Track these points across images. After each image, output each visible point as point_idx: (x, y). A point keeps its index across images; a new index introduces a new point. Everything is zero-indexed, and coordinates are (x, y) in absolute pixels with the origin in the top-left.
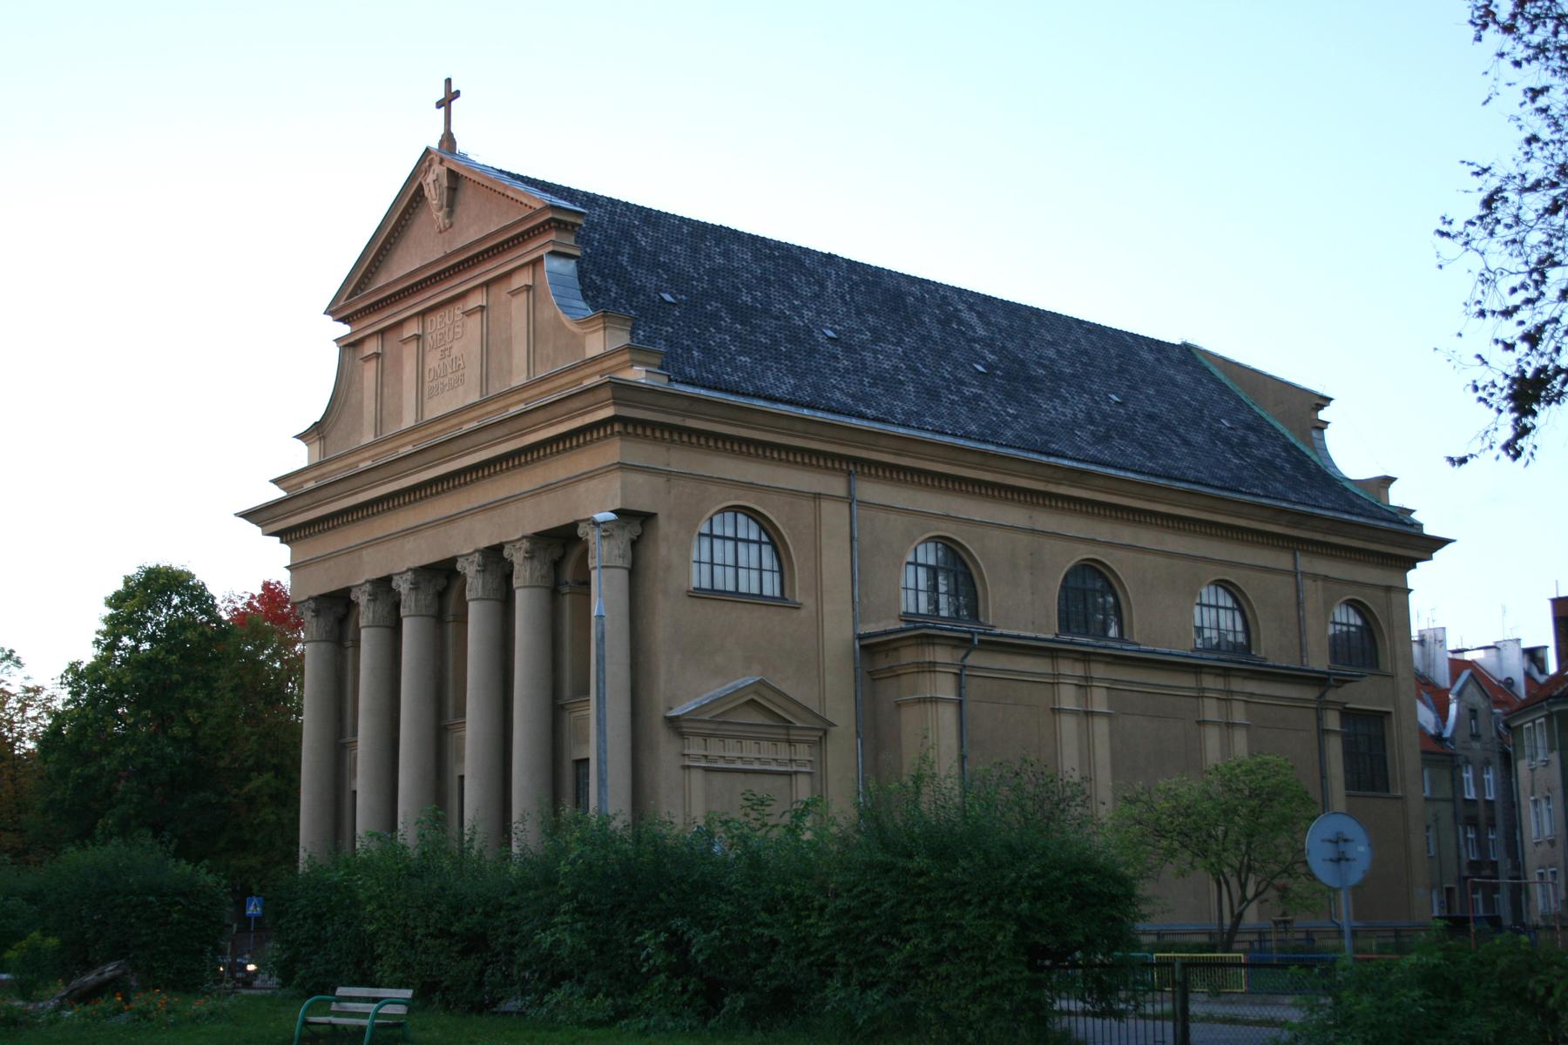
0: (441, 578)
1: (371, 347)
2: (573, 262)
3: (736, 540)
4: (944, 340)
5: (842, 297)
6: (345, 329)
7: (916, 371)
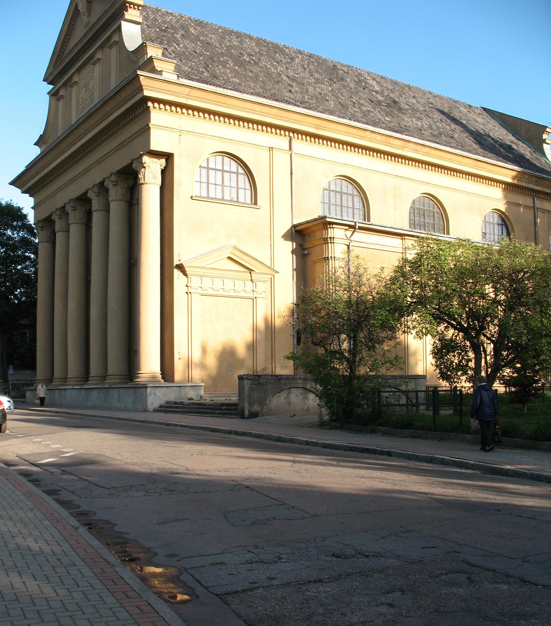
0: (83, 200)
1: (62, 93)
2: (139, 26)
3: (223, 171)
4: (356, 88)
5: (303, 66)
6: (51, 87)
7: (337, 97)
